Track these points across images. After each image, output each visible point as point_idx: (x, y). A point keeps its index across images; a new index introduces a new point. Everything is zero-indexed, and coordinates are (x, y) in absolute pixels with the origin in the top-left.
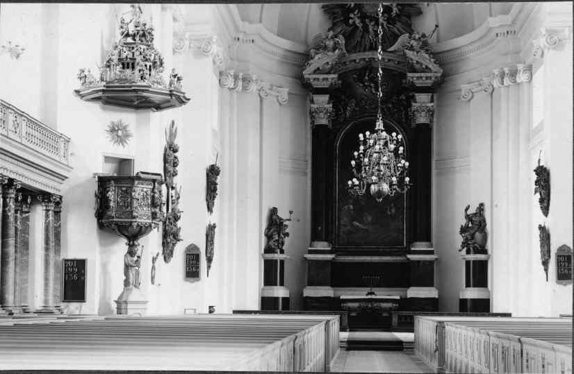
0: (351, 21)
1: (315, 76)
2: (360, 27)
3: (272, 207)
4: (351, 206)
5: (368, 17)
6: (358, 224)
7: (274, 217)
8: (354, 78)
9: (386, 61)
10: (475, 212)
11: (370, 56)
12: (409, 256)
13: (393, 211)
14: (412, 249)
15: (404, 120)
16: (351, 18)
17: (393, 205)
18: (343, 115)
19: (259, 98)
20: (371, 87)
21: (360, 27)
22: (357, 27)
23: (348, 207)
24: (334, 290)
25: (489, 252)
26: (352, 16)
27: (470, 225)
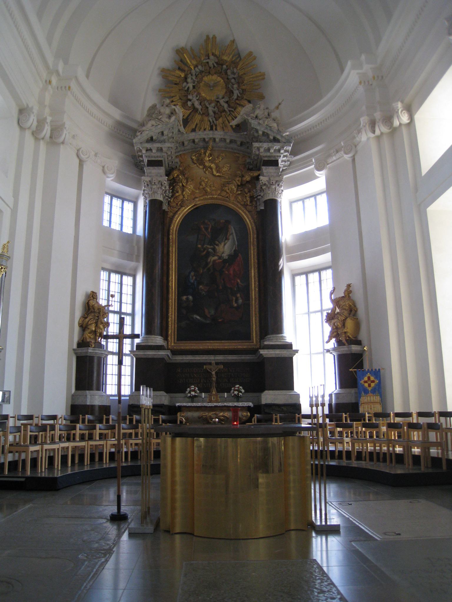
0: (189, 103)
1: (149, 146)
2: (200, 110)
3: (90, 290)
4: (191, 297)
5: (205, 99)
6: (198, 317)
7: (92, 303)
8: (192, 159)
9: (228, 141)
10: (343, 295)
11: (211, 136)
12: (262, 352)
13: (240, 301)
14: (266, 343)
15: (248, 203)
16: (190, 100)
17: (238, 295)
18: (181, 197)
19: (77, 161)
20: (211, 168)
21: (200, 110)
22: (195, 110)
23: (187, 299)
24: (171, 397)
25: (365, 342)
26: (190, 97)
27: (338, 310)
